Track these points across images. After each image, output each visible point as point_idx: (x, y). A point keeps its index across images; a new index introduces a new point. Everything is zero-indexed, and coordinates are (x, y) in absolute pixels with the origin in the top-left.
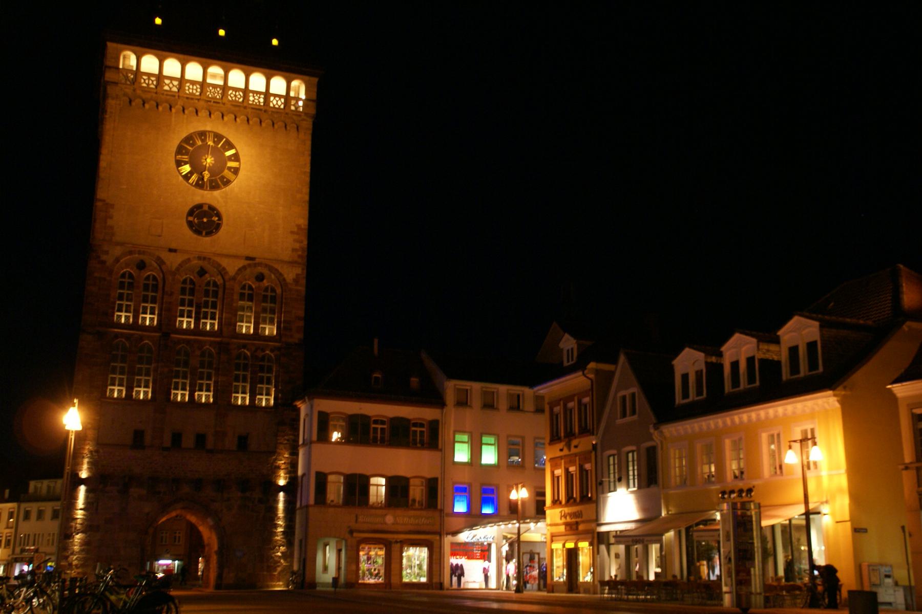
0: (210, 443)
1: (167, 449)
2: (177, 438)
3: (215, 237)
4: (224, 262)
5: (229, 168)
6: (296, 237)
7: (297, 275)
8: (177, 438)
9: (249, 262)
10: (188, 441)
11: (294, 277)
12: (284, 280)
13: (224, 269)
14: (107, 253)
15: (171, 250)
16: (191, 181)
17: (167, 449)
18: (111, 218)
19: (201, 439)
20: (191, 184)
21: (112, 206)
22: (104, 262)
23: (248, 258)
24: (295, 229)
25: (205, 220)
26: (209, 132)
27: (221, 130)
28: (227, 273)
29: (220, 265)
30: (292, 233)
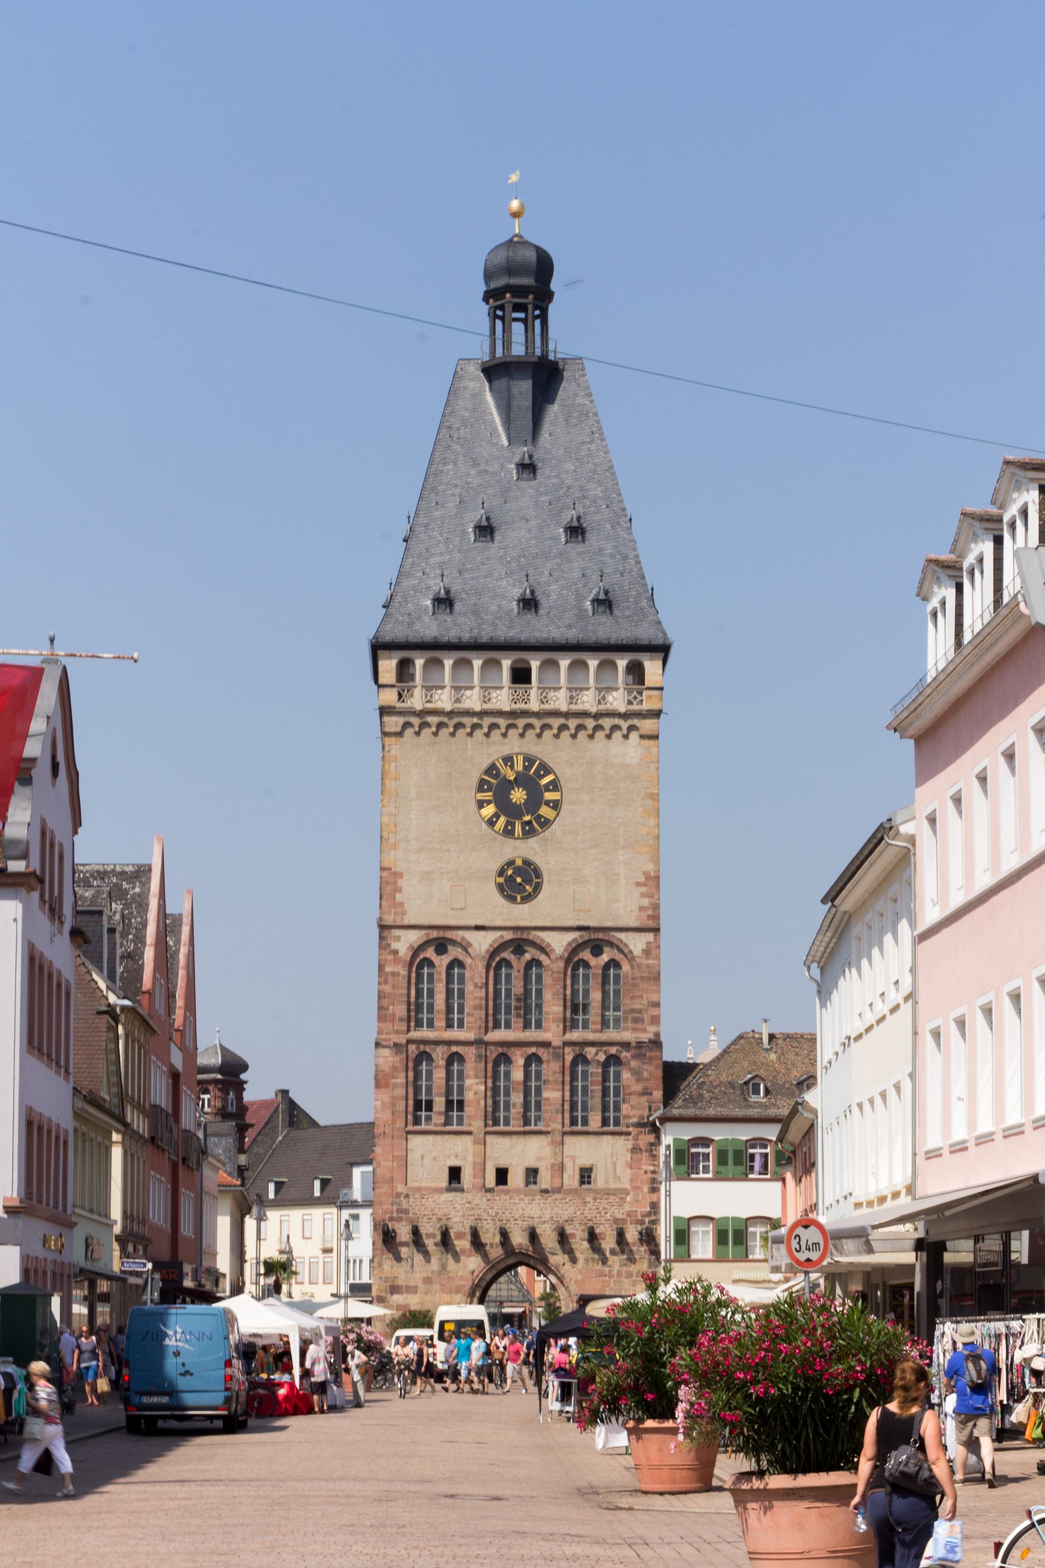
0: (545, 1179)
1: (489, 1190)
2: (502, 1176)
3: (533, 902)
4: (547, 937)
5: (547, 803)
6: (644, 889)
7: (648, 943)
8: (502, 1176)
9: (582, 933)
10: (516, 1178)
11: (644, 947)
12: (631, 952)
13: (549, 945)
15: (479, 928)
16: (497, 827)
17: (489, 1190)
18: (400, 890)
19: (532, 1174)
20: (498, 833)
21: (400, 875)
22: (395, 952)
24: (642, 879)
25: (519, 880)
26: (517, 754)
28: (553, 950)
29: (543, 940)
30: (638, 884)
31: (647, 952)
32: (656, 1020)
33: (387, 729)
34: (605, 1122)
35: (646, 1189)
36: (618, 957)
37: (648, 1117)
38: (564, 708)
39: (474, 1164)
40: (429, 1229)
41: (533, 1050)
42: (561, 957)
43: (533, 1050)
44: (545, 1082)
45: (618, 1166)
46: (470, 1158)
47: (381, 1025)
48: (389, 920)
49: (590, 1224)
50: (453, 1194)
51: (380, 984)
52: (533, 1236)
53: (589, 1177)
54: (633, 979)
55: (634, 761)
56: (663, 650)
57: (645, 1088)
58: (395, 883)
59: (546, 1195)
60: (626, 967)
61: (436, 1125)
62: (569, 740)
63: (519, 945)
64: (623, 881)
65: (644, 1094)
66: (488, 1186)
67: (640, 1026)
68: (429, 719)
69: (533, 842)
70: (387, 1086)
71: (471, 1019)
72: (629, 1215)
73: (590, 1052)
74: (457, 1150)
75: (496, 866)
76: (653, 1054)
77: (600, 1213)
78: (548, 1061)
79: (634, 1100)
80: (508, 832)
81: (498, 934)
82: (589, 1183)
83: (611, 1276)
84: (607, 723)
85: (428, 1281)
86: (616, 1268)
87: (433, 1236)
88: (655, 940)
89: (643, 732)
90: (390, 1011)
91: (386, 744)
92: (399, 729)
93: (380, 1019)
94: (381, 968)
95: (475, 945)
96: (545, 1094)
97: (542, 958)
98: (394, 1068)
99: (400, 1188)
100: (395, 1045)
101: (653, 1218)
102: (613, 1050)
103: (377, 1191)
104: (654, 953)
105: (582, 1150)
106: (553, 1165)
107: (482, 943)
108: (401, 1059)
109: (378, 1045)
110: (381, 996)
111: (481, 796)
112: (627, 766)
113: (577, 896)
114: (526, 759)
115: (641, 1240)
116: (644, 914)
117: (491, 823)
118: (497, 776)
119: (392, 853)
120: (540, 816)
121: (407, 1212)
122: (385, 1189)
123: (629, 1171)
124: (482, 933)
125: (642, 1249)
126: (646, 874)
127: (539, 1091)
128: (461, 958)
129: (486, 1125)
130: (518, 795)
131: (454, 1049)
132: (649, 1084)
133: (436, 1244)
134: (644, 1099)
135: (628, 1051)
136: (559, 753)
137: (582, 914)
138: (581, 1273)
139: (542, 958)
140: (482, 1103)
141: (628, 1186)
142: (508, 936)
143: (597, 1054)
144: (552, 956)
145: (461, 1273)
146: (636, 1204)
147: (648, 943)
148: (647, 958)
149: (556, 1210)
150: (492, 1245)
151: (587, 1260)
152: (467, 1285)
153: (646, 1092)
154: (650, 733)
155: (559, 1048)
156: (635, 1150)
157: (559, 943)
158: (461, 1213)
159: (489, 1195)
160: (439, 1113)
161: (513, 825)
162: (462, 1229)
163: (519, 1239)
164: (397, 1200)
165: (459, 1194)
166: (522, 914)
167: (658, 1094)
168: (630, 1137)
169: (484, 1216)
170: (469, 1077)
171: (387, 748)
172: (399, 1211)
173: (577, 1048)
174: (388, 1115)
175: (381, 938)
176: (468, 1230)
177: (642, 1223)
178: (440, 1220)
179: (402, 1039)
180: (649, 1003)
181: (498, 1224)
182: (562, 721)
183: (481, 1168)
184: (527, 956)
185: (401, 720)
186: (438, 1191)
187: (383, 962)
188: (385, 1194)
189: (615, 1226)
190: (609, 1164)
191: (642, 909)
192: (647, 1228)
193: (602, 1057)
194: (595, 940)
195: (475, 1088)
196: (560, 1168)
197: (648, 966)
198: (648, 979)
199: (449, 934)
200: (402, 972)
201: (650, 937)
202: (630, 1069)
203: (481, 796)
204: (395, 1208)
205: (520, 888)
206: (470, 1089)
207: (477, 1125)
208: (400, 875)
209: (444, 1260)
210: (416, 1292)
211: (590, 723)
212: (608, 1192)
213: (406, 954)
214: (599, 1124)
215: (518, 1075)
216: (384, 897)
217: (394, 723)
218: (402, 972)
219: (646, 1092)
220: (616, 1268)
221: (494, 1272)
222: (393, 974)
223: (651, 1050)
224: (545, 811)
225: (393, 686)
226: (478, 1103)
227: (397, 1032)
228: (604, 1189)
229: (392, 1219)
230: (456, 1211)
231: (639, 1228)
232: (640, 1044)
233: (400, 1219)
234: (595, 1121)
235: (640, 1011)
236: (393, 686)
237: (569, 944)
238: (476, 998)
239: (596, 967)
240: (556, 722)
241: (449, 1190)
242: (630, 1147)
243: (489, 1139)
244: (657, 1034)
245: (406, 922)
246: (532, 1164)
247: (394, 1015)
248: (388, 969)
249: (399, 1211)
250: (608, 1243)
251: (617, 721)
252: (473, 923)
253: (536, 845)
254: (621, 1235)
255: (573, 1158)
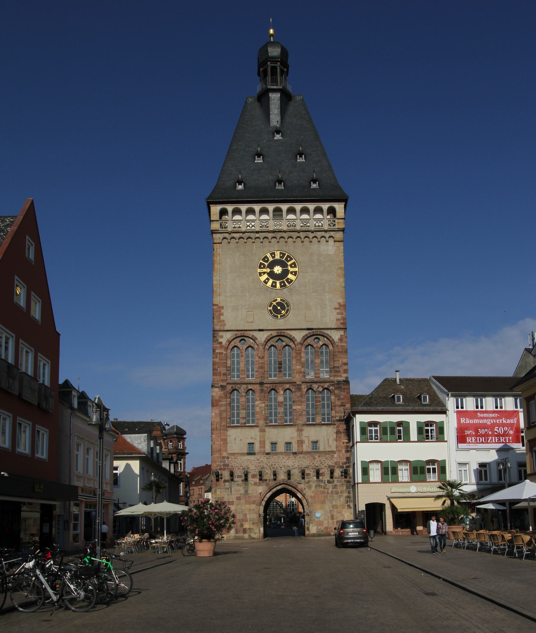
4: (293, 334)
6: (338, 311)
7: (341, 336)
10: (281, 448)
11: (339, 337)
12: (333, 340)
13: (294, 338)
14: (222, 337)
16: (268, 285)
17: (268, 454)
18: (222, 315)
21: (223, 308)
22: (221, 343)
23: (308, 329)
24: (338, 306)
25: (279, 308)
27: (285, 249)
28: (296, 340)
29: (291, 335)
30: (336, 309)
31: (341, 340)
32: (346, 371)
33: (215, 241)
34: (323, 420)
35: (344, 451)
36: (328, 342)
37: (344, 417)
38: (298, 228)
39: (260, 442)
40: (238, 472)
41: (287, 386)
42: (300, 343)
43: (287, 386)
44: (294, 401)
45: (330, 441)
46: (258, 439)
47: (214, 377)
48: (217, 328)
49: (317, 468)
50: (250, 456)
51: (213, 358)
52: (289, 474)
53: (316, 446)
54: (334, 352)
55: (332, 253)
56: (344, 200)
57: (342, 403)
58: (220, 311)
59: (295, 456)
60: (331, 347)
61: (241, 424)
62: (300, 244)
63: (280, 339)
64: (328, 307)
65: (342, 406)
66: (267, 452)
67: (338, 374)
68: (235, 235)
69: (285, 290)
70: (217, 406)
71: (257, 374)
72: (336, 464)
73: (315, 386)
74: (252, 435)
75: (268, 302)
76: (345, 387)
77: (322, 463)
78: (295, 392)
79: (337, 408)
80: (274, 286)
81: (269, 333)
82: (316, 449)
83: (328, 493)
84: (319, 234)
85: (239, 498)
86: (330, 490)
87: (241, 477)
88: (345, 334)
89: (335, 239)
90: (219, 371)
91: (215, 248)
92: (220, 241)
93: (214, 374)
94: (214, 351)
95: (259, 338)
96: (294, 408)
97: (291, 344)
98: (220, 397)
99: (225, 454)
100: (221, 386)
101: (348, 465)
102: (326, 386)
103: (213, 456)
104: (344, 340)
105: (311, 433)
106: (298, 441)
107: (262, 337)
108: (224, 393)
109: (213, 386)
110: (214, 364)
111: (259, 270)
112: (329, 255)
113: (307, 315)
114: (280, 253)
115: (342, 476)
116: (339, 322)
117: (266, 282)
118: (267, 262)
119: (218, 298)
120: (288, 279)
121: (228, 465)
122: (217, 455)
123: (335, 442)
124: (262, 332)
125: (343, 480)
126: (340, 304)
127: (291, 406)
128: (252, 345)
129: (266, 423)
130: (278, 270)
131: (250, 388)
132: (343, 401)
133: (242, 481)
134: (342, 409)
135: (333, 385)
136: (297, 250)
137: (309, 323)
138: (313, 492)
139: (291, 344)
140: (264, 412)
141: (335, 449)
142: (274, 333)
143: (318, 388)
144: (296, 343)
145: (254, 494)
146: (340, 458)
147: (341, 336)
148: (341, 343)
149: (301, 462)
150: (270, 480)
151: (316, 486)
152: (258, 500)
153: (343, 405)
154: (339, 240)
155: (300, 385)
156: (338, 432)
157: (298, 336)
158: (254, 465)
159: (268, 456)
160: (243, 418)
161: (276, 283)
162: (255, 473)
163: (282, 477)
164: (223, 460)
165: (253, 456)
166: (280, 323)
167: (348, 406)
168: (335, 427)
169: (265, 466)
170: (257, 400)
171: (215, 250)
172: (224, 465)
173: (309, 384)
174: (218, 420)
175: (214, 337)
176: (258, 473)
177: (342, 467)
178: (244, 468)
179: (225, 384)
180: (342, 363)
181: (273, 470)
182: (297, 234)
183: (263, 443)
184: (284, 344)
185: (221, 236)
186: (242, 454)
187: (214, 348)
188: (217, 457)
189: (329, 469)
190: (326, 440)
191: (338, 320)
192: (345, 470)
193: (321, 389)
194: (316, 333)
195: (260, 405)
196: (301, 443)
197: (341, 346)
198: (342, 352)
199: (246, 333)
200: (224, 352)
201: (342, 332)
202: (335, 394)
203: (259, 270)
204: (222, 464)
205: (279, 312)
206: (257, 406)
207: (261, 423)
208: (223, 308)
209: (246, 488)
210: (233, 505)
211: (311, 235)
212: (326, 453)
213: (226, 344)
214: (320, 420)
215: (281, 399)
216: (215, 318)
217: (217, 237)
218: (224, 352)
219: (343, 405)
220: (330, 490)
221: (270, 493)
222: (220, 353)
223: (344, 385)
224: (290, 276)
225: (217, 221)
226: (262, 412)
227: (223, 380)
228: (324, 452)
229: (220, 469)
230: (252, 464)
231: (341, 470)
232: (339, 382)
233: (224, 469)
234: (319, 420)
235: (338, 367)
236: (217, 221)
237: (304, 337)
238: (259, 363)
239: (317, 347)
240: (295, 235)
241: (249, 454)
242: (335, 431)
243: (267, 429)
244: (347, 378)
245: (226, 329)
246: (288, 440)
247: (220, 372)
248: (217, 351)
249: (224, 465)
250: (326, 477)
251: (323, 234)
252: (258, 329)
253: (286, 292)
254: (332, 472)
255: (308, 437)
